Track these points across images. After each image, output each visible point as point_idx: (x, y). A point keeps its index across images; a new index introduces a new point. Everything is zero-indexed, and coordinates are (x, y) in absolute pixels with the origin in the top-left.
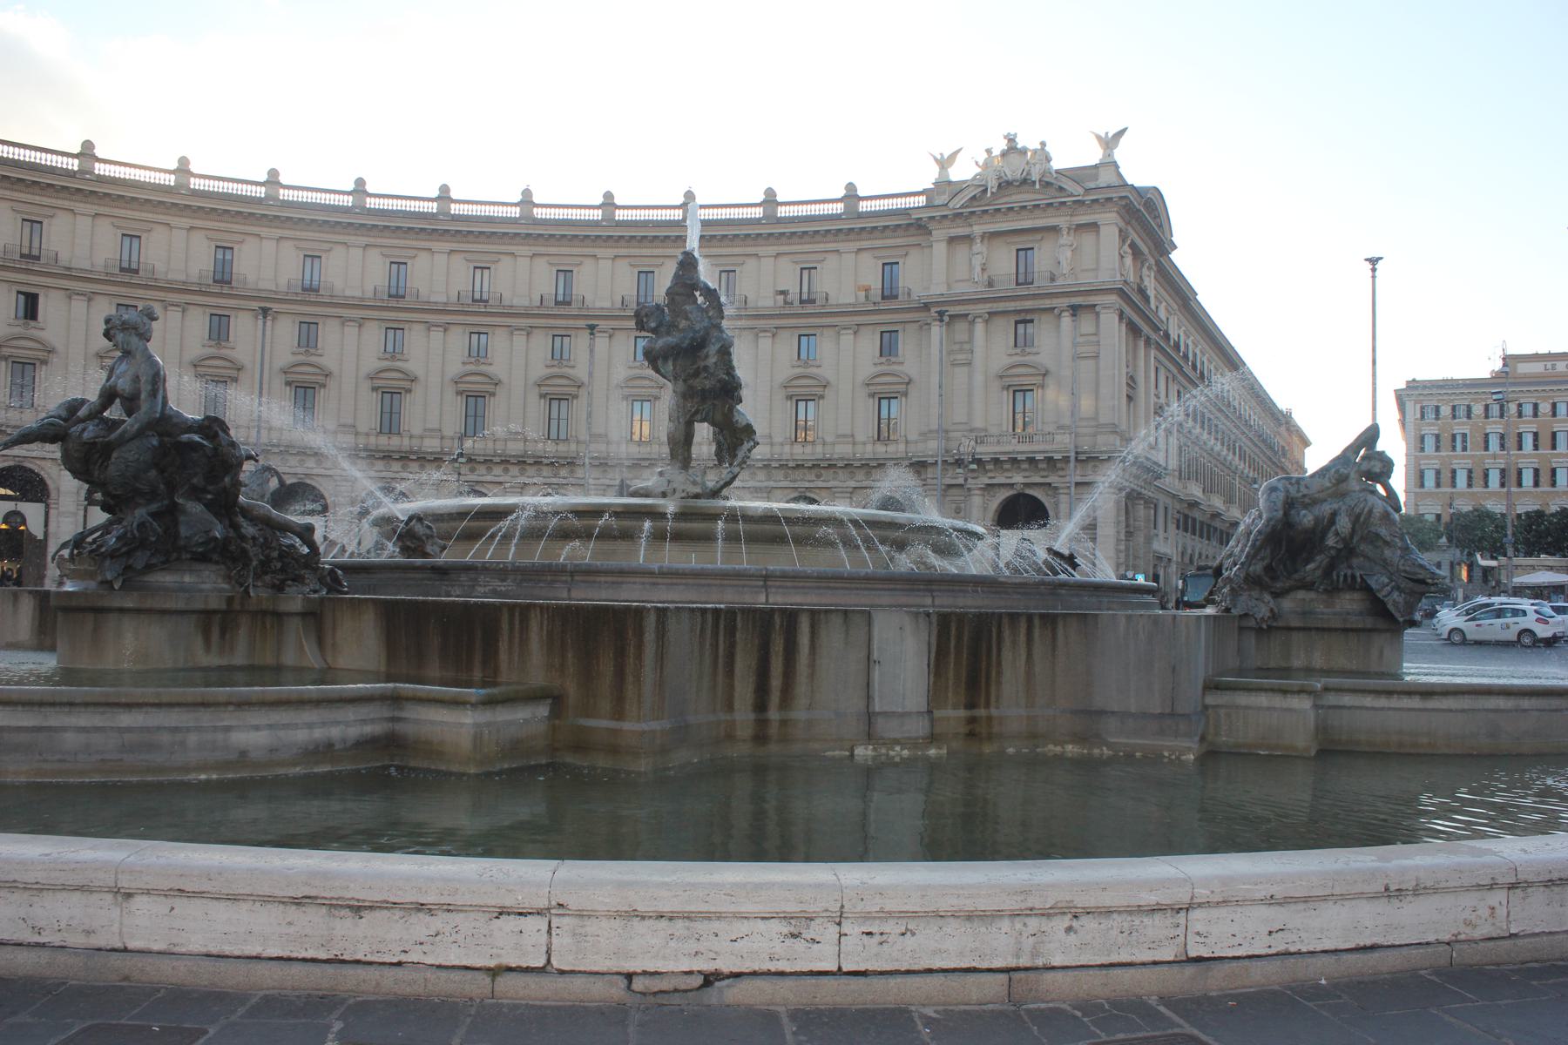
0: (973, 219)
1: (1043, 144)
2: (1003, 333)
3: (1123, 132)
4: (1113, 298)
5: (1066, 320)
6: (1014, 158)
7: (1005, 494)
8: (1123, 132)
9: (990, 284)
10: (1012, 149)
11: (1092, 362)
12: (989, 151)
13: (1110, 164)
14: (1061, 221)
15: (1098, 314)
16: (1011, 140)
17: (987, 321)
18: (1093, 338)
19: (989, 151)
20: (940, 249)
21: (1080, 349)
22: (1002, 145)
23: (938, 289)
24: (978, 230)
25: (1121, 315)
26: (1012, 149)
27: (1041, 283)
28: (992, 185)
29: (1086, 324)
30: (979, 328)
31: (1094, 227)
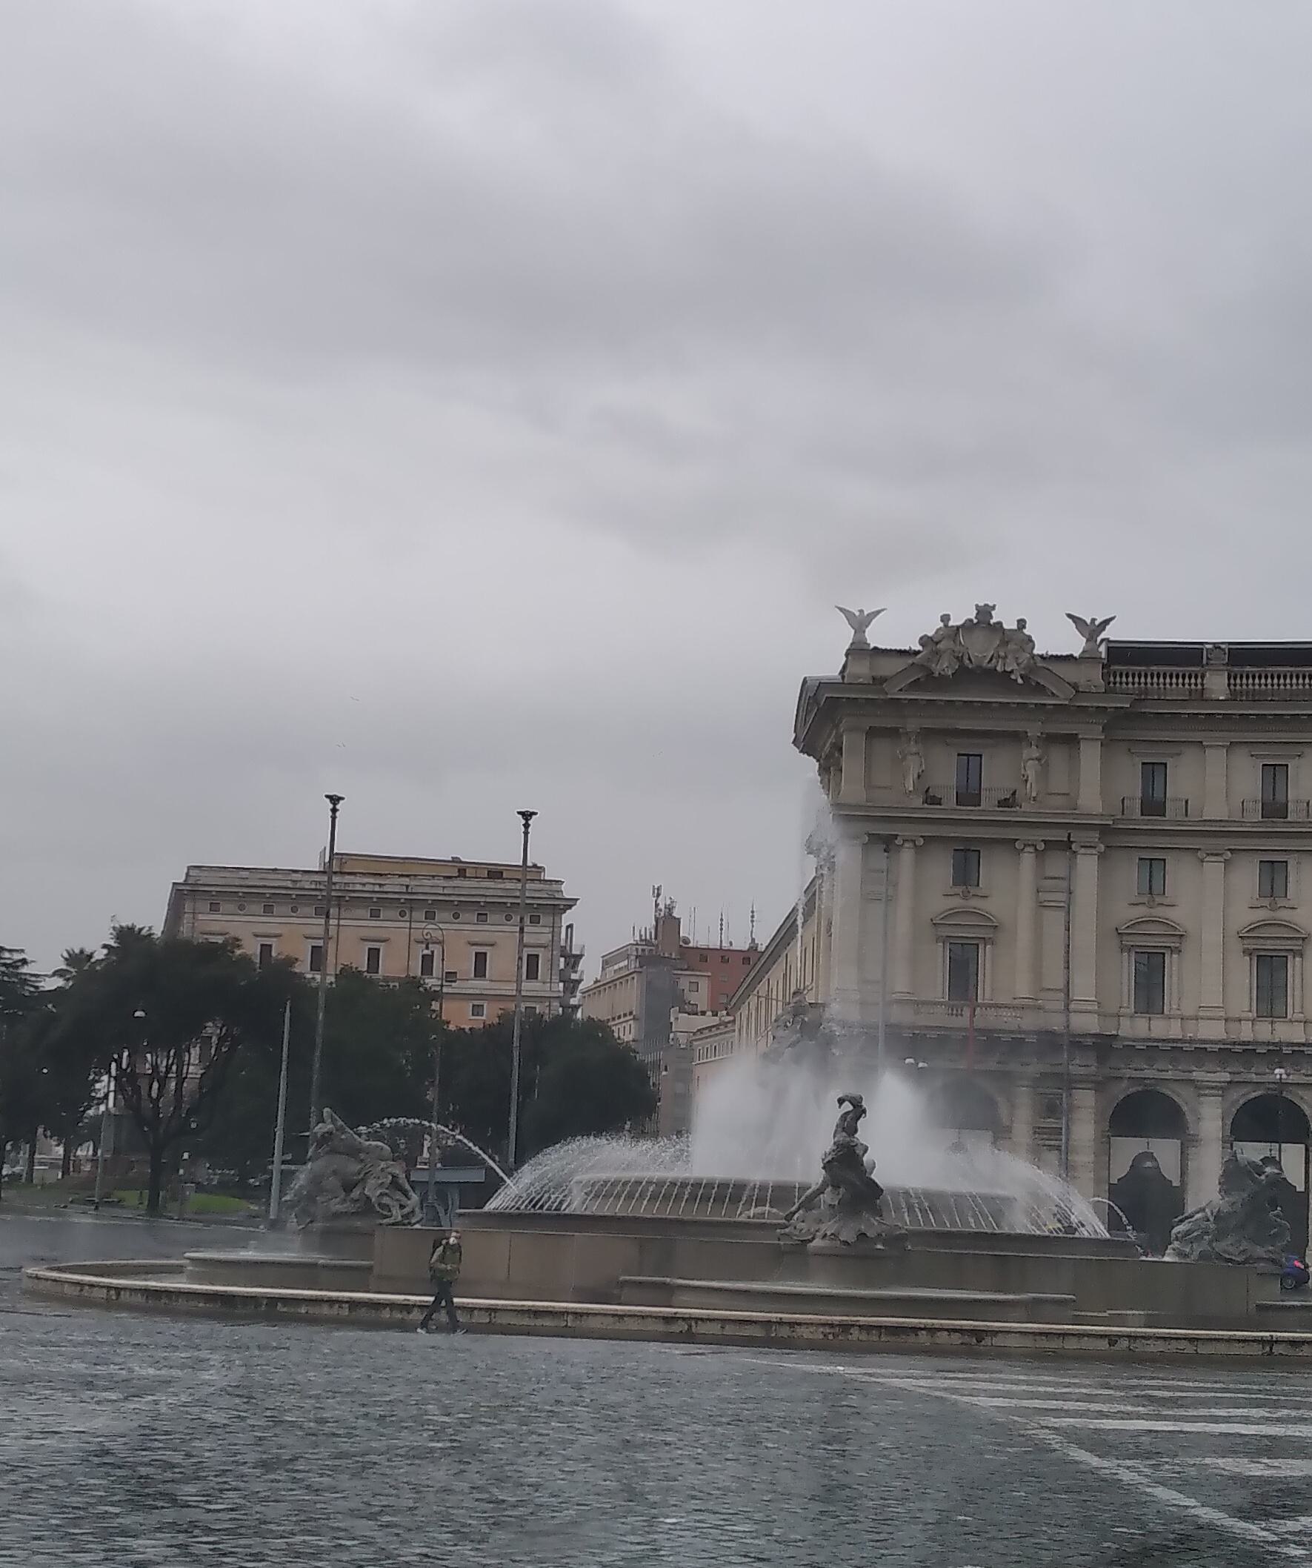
1: (1022, 624)
2: (941, 869)
5: (1028, 859)
12: (945, 618)
14: (1034, 730)
18: (1064, 884)
19: (945, 618)
21: (1043, 896)
24: (913, 725)
28: (945, 667)
31: (1071, 741)
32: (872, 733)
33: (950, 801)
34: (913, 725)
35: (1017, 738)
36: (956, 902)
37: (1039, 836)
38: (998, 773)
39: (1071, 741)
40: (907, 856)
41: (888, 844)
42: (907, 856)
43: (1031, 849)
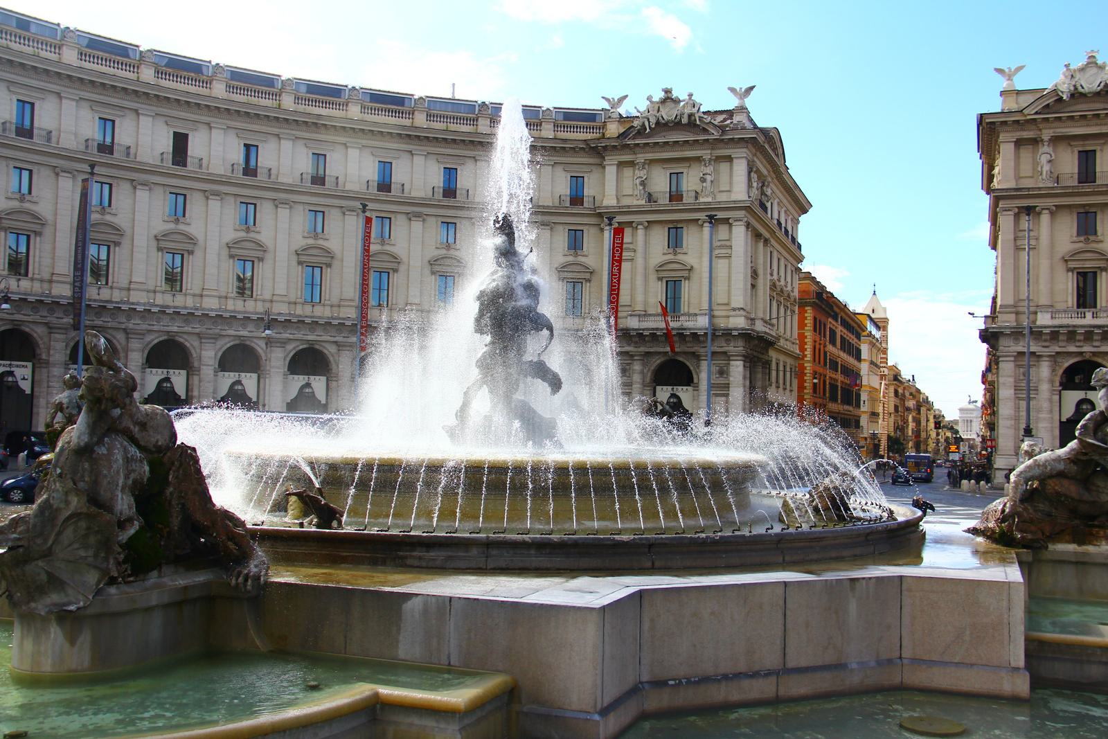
0: (637, 149)
1: (690, 95)
2: (659, 237)
3: (752, 88)
4: (741, 214)
6: (669, 104)
7: (658, 361)
8: (752, 88)
9: (650, 198)
10: (668, 98)
11: (726, 261)
12: (649, 98)
13: (742, 109)
14: (705, 153)
15: (731, 225)
16: (668, 91)
17: (646, 228)
20: (611, 171)
22: (662, 95)
23: (610, 201)
24: (641, 158)
25: (748, 225)
26: (668, 98)
27: (688, 199)
29: (722, 231)
30: (641, 232)
31: (729, 159)
32: (621, 164)
33: (664, 200)
34: (1046, 134)
35: (698, 159)
36: (571, 259)
37: (1050, 202)
38: (691, 181)
39: (729, 159)
40: (1045, 218)
41: (1029, 210)
42: (1045, 218)
43: (1047, 211)
